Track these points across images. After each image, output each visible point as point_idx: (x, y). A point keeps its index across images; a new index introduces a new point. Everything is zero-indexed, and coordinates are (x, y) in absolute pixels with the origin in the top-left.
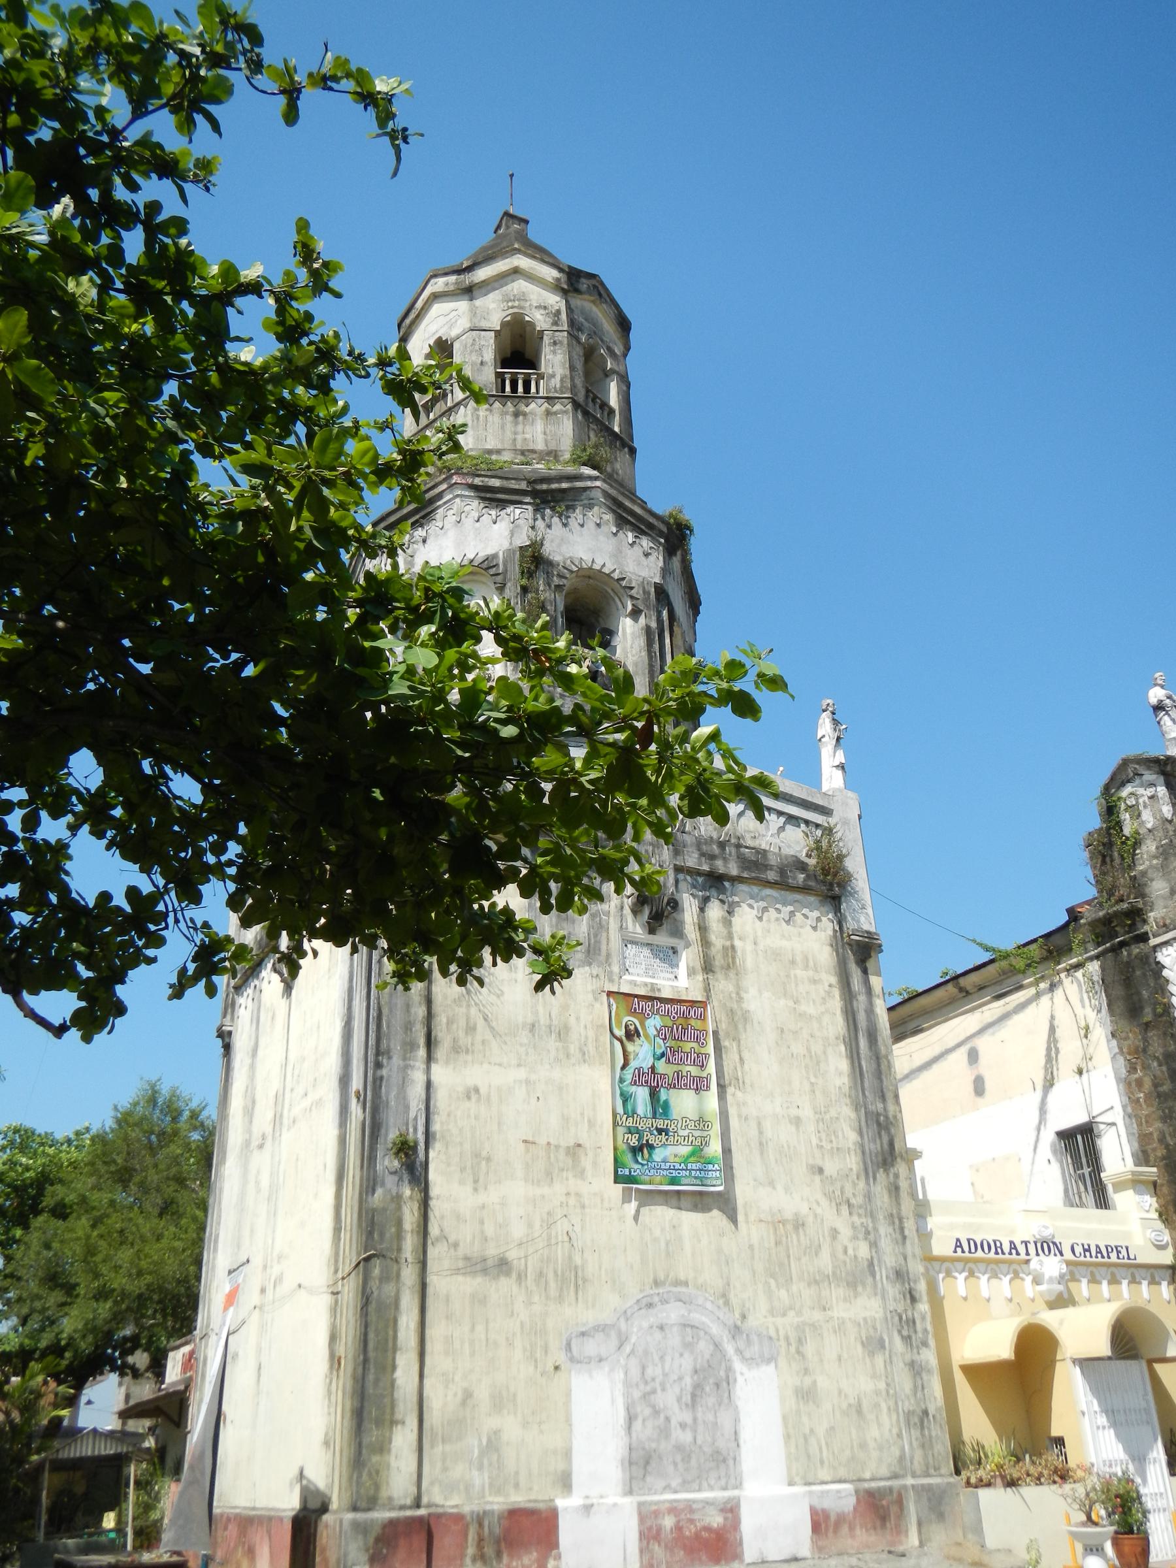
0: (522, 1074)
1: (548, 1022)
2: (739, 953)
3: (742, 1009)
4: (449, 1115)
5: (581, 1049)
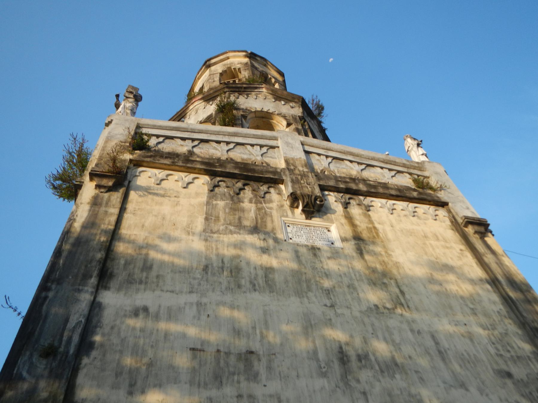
0: (194, 298)
1: (220, 265)
2: (381, 230)
3: (392, 261)
4: (112, 328)
5: (251, 282)
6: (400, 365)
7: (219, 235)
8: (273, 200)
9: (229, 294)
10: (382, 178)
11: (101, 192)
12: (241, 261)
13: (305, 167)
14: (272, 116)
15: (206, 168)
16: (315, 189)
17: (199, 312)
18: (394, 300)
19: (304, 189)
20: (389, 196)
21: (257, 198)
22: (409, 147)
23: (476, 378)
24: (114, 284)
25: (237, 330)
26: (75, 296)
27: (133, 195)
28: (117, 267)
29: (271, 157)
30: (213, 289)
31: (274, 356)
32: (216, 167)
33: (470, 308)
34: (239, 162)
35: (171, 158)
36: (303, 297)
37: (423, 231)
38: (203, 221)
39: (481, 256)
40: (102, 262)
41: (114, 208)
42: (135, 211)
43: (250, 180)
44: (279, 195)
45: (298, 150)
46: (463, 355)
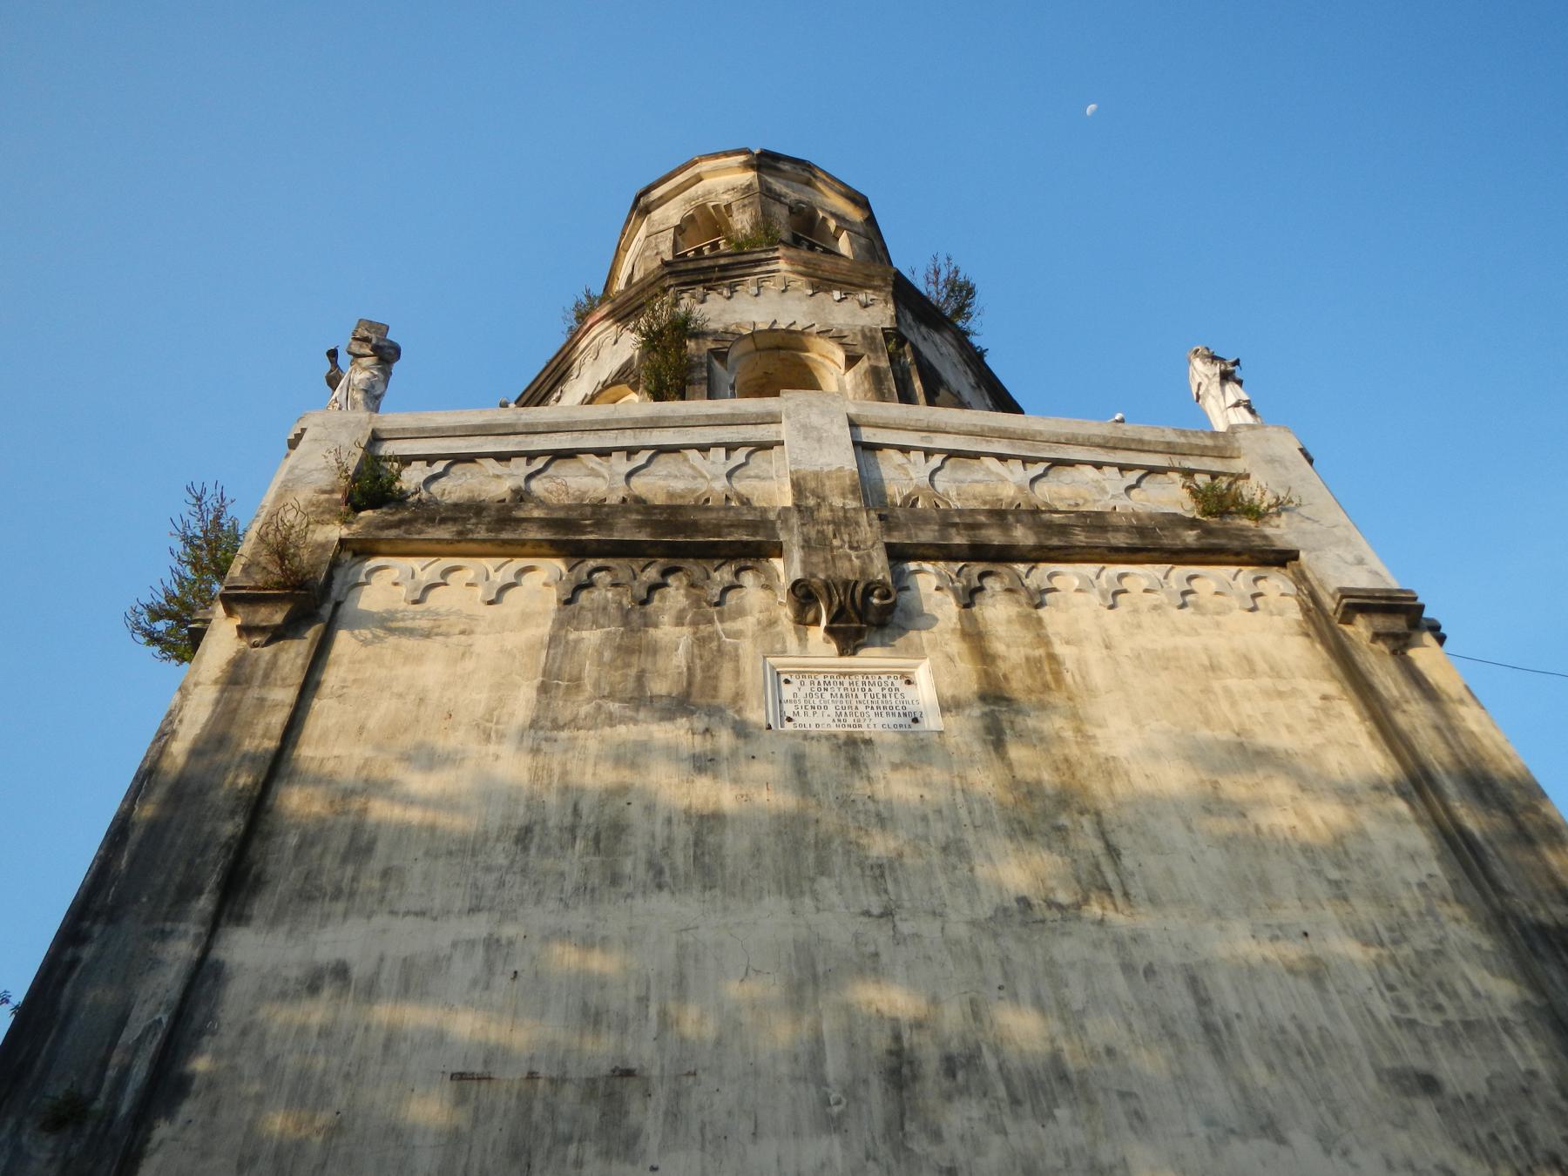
0: (479, 927)
1: (568, 820)
2: (1070, 664)
3: (1092, 755)
4: (244, 1033)
5: (651, 864)
6: (1074, 1077)
7: (576, 733)
8: (747, 607)
9: (582, 903)
10: (1097, 497)
11: (255, 645)
12: (629, 804)
13: (850, 496)
14: (804, 339)
15: (553, 537)
16: (871, 560)
17: (489, 966)
18: (1084, 876)
19: (839, 564)
20: (1106, 552)
21: (699, 607)
22: (1200, 385)
23: (1315, 1102)
24: (261, 906)
25: (593, 1010)
26: (151, 951)
27: (344, 641)
28: (276, 856)
29: (757, 477)
30: (539, 893)
31: (691, 1079)
32: (582, 529)
33: (1330, 881)
34: (656, 507)
35: (454, 520)
36: (802, 893)
37: (1206, 649)
38: (534, 694)
39: (1385, 712)
40: (235, 846)
41: (284, 686)
42: (343, 687)
43: (685, 556)
44: (768, 592)
45: (838, 444)
46: (1283, 1030)
